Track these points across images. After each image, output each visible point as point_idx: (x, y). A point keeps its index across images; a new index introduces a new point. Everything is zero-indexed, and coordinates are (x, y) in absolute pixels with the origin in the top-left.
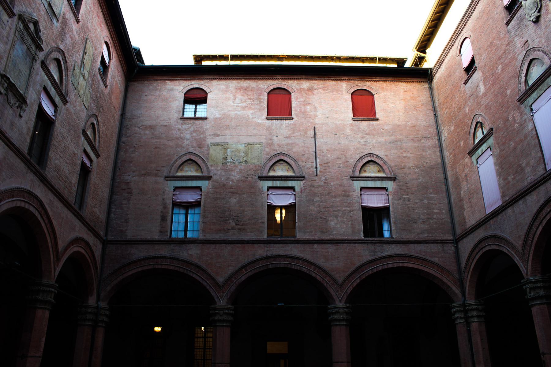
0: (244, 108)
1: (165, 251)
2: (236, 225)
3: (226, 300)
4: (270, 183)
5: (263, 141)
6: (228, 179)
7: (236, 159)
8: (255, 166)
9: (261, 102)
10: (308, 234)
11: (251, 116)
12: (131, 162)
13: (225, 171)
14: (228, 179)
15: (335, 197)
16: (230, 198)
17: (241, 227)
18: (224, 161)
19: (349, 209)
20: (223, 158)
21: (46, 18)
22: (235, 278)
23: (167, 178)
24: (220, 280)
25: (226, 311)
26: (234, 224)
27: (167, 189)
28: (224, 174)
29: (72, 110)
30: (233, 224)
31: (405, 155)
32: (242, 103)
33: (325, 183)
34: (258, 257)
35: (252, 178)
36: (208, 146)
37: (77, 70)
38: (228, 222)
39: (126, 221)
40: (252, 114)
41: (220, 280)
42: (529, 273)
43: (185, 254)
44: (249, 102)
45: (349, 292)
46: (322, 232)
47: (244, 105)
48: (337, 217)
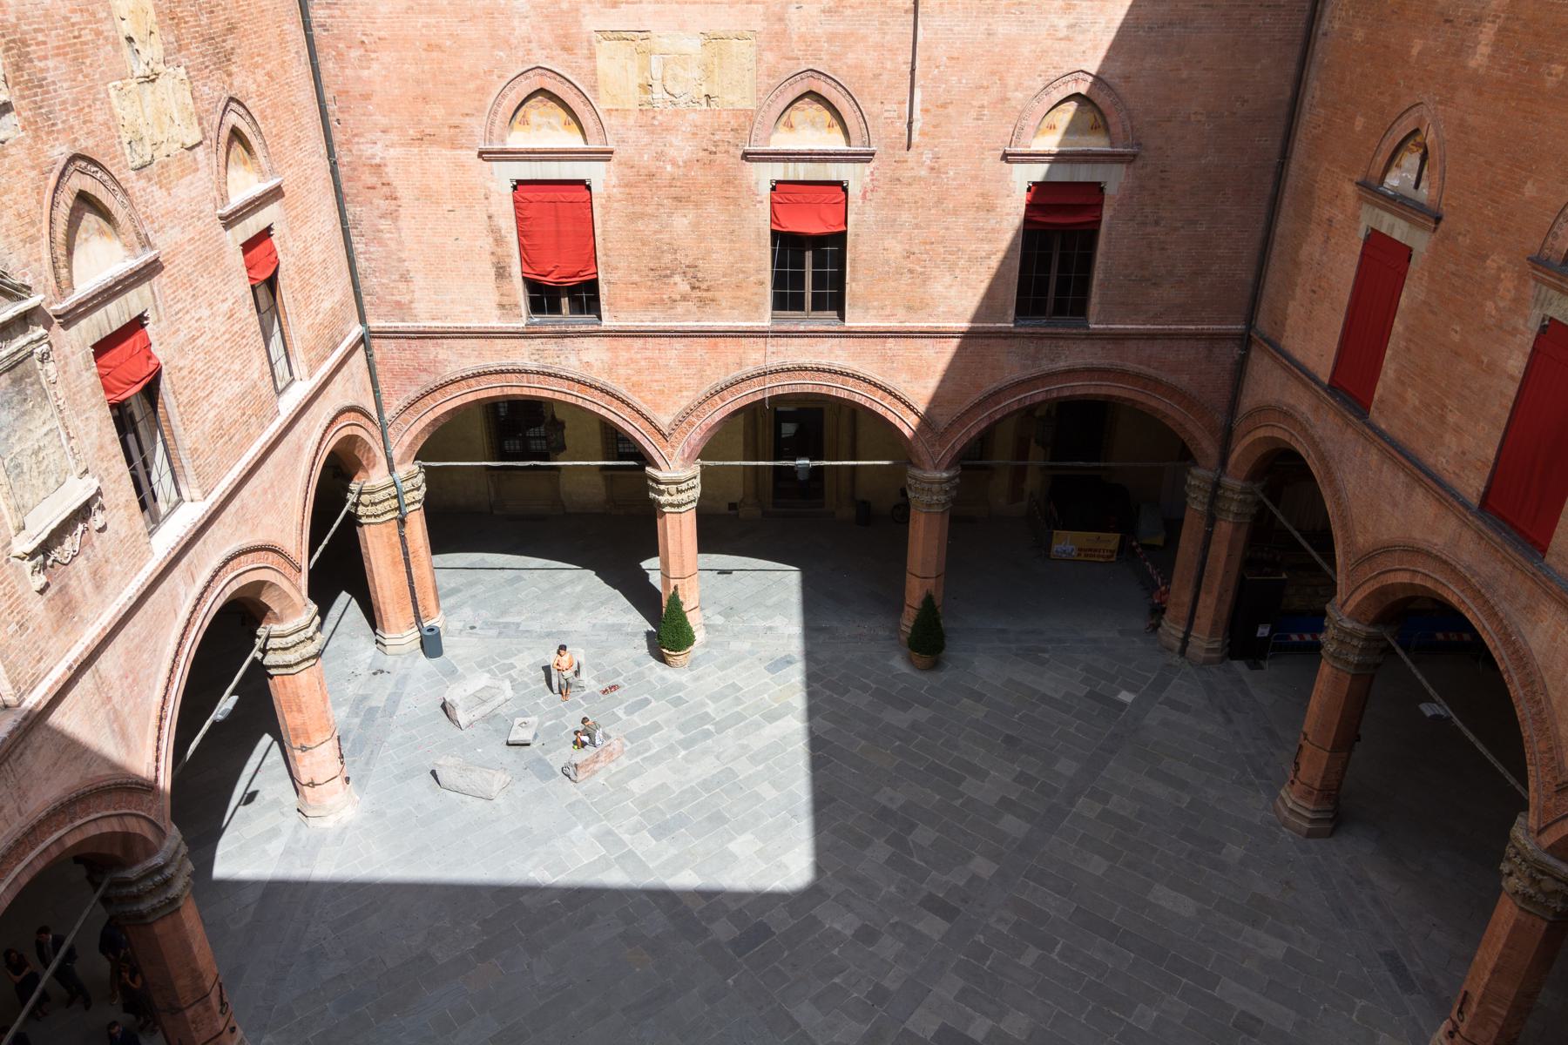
2: (693, 288)
4: (780, 171)
6: (660, 156)
7: (676, 91)
8: (736, 113)
10: (873, 312)
12: (366, 97)
13: (650, 129)
14: (660, 156)
15: (955, 212)
16: (670, 215)
18: (645, 97)
19: (986, 247)
20: (641, 86)
26: (688, 287)
27: (493, 186)
28: (646, 139)
30: (684, 287)
31: (1185, 74)
33: (932, 169)
35: (727, 152)
36: (589, 42)
38: (672, 281)
39: (405, 278)
41: (664, 420)
42: (1349, 608)
43: (573, 360)
45: (958, 447)
46: (910, 308)
48: (951, 269)
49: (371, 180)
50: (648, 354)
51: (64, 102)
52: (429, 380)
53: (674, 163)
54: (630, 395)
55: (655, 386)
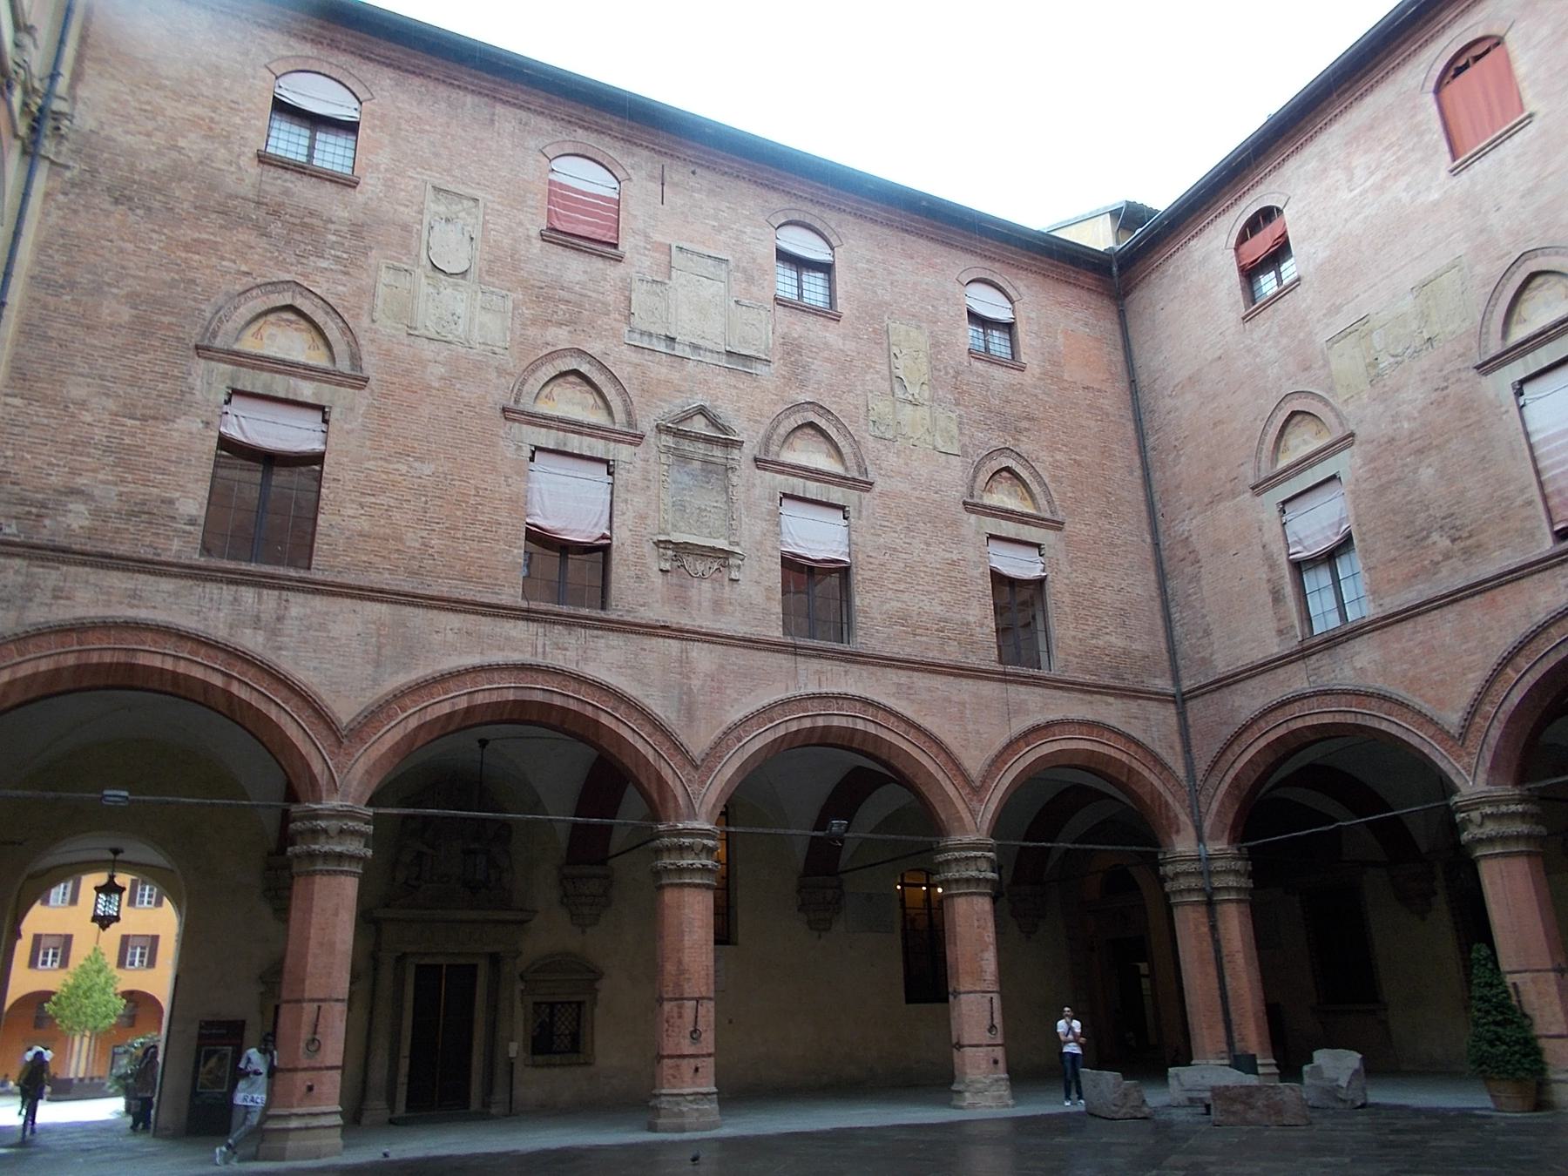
0: (1380, 188)
1: (1297, 680)
2: (1454, 541)
3: (1482, 776)
4: (1518, 370)
5: (1461, 249)
6: (1395, 419)
7: (1399, 350)
9: (1421, 134)
11: (1405, 197)
12: (1178, 487)
16: (1415, 471)
17: (1468, 542)
21: (733, 381)
22: (1492, 702)
23: (1258, 488)
24: (1452, 719)
25: (1488, 810)
26: (1448, 542)
27: (1264, 516)
28: (1381, 408)
29: (904, 487)
32: (1372, 173)
34: (1541, 617)
36: (1322, 351)
37: (881, 407)
38: (1430, 541)
39: (1207, 633)
40: (1408, 188)
43: (1348, 672)
44: (1389, 157)
47: (1377, 177)
49: (1181, 552)
50: (1420, 637)
51: (819, 382)
52: (1227, 732)
53: (1410, 418)
54: (1409, 696)
55: (1435, 676)
